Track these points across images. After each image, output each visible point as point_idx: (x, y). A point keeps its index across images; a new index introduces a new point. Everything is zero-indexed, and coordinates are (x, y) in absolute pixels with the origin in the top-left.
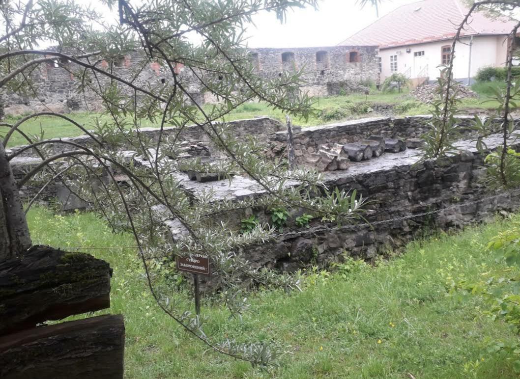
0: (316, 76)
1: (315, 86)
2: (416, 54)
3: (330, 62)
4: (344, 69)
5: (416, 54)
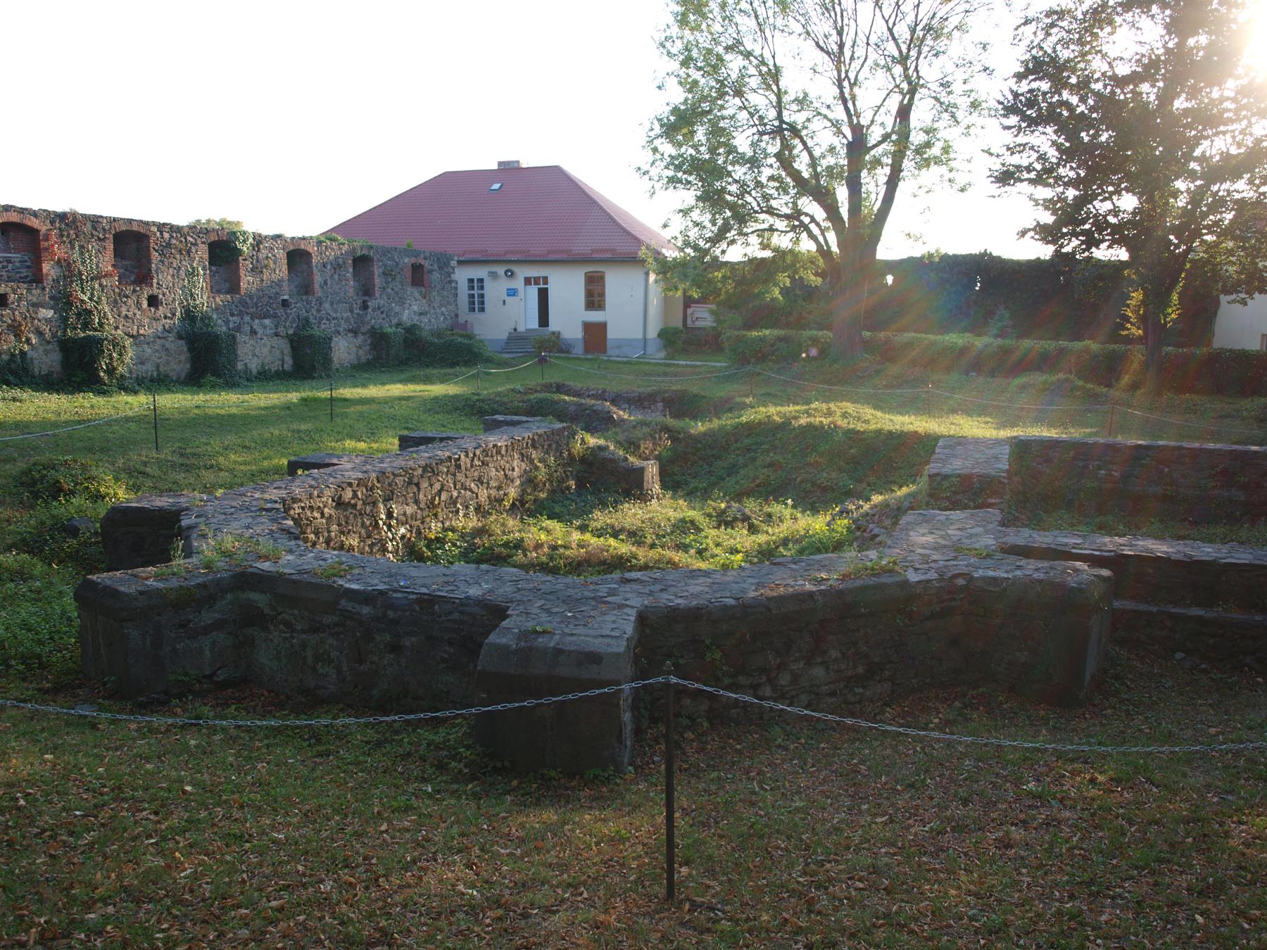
0: (351, 311)
3: (378, 281)
4: (402, 302)
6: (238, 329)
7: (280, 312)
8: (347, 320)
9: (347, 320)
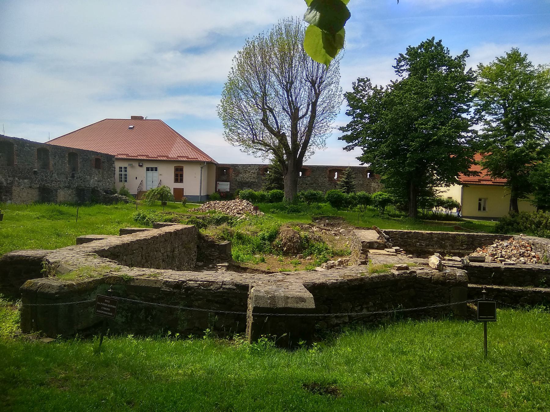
0: (67, 179)
1: (66, 189)
2: (148, 169)
4: (90, 175)
5: (148, 169)
6: (12, 183)
7: (33, 176)
8: (65, 182)
9: (65, 182)
